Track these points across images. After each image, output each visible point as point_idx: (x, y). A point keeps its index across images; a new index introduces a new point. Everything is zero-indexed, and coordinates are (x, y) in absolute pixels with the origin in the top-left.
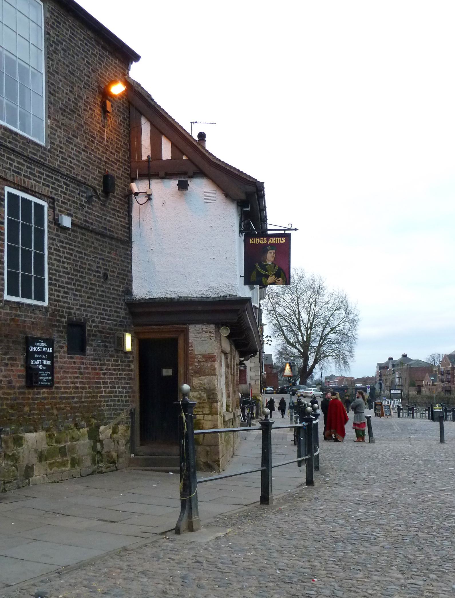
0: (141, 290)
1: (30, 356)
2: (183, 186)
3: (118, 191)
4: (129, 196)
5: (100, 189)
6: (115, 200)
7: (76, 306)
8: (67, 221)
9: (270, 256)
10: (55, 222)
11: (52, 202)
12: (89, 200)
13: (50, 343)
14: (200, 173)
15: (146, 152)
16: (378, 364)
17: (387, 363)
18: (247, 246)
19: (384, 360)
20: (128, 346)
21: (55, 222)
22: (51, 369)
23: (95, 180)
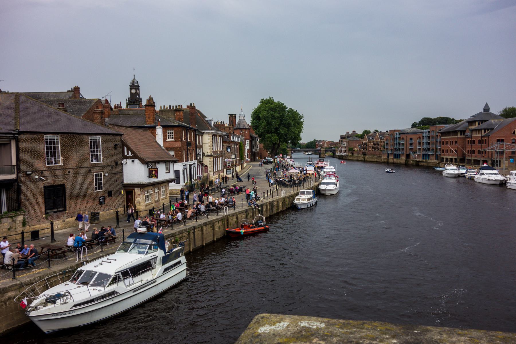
0: (126, 181)
1: (100, 200)
2: (133, 161)
3: (119, 163)
4: (122, 164)
5: (114, 165)
6: (119, 165)
7: (109, 189)
8: (107, 175)
9: (154, 172)
10: (104, 175)
11: (103, 172)
12: (112, 168)
13: (104, 197)
14: (136, 158)
15: (126, 154)
16: (341, 136)
17: (346, 135)
18: (149, 170)
19: (344, 134)
20: (122, 193)
21: (104, 175)
22: (104, 201)
23: (113, 163)
